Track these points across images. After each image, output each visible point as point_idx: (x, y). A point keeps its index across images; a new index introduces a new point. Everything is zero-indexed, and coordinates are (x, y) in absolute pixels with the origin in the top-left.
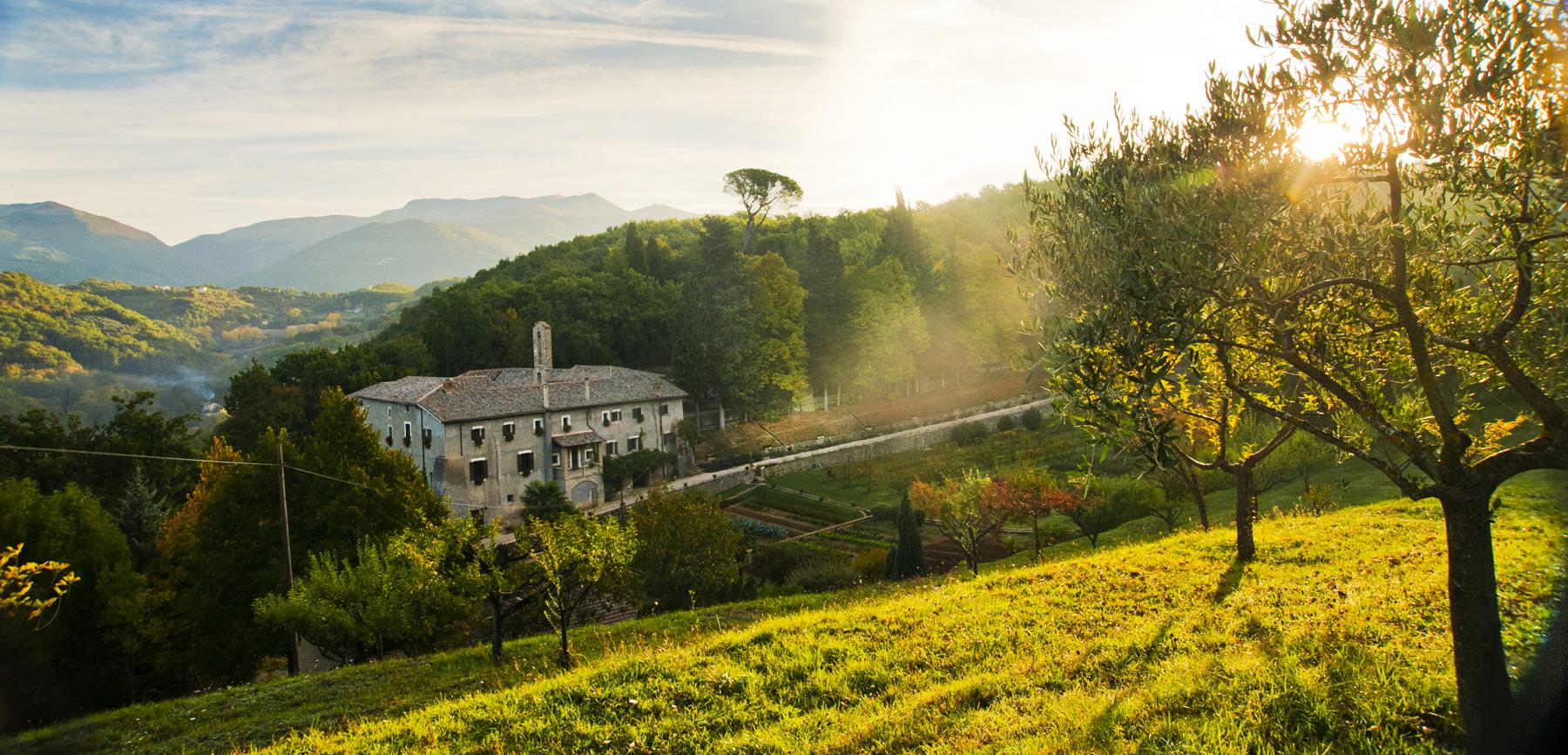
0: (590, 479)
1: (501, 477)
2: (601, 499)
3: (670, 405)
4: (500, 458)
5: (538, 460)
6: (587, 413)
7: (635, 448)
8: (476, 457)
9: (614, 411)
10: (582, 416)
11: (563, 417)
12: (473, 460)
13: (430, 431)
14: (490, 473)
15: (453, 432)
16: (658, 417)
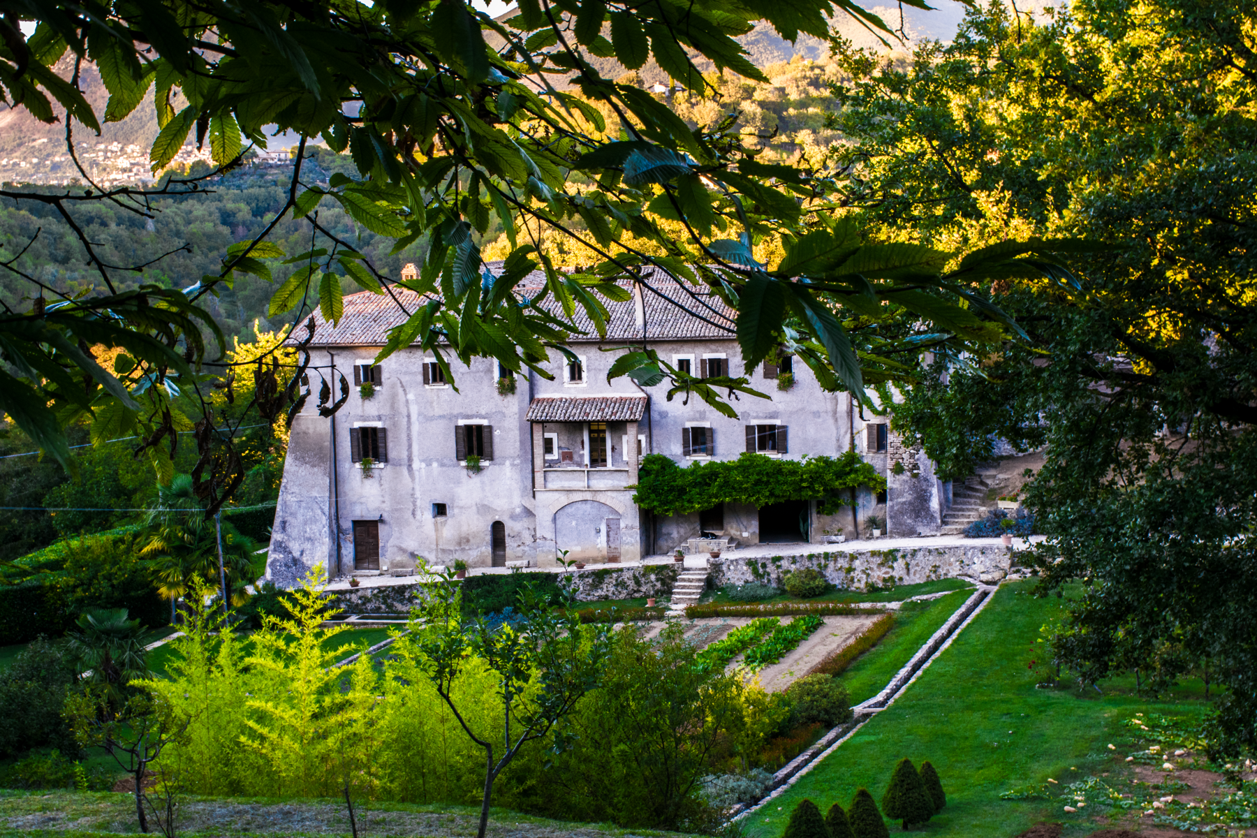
0: (601, 498)
1: (416, 465)
4: (415, 428)
5: (507, 438)
8: (364, 419)
12: (357, 425)
14: (392, 454)
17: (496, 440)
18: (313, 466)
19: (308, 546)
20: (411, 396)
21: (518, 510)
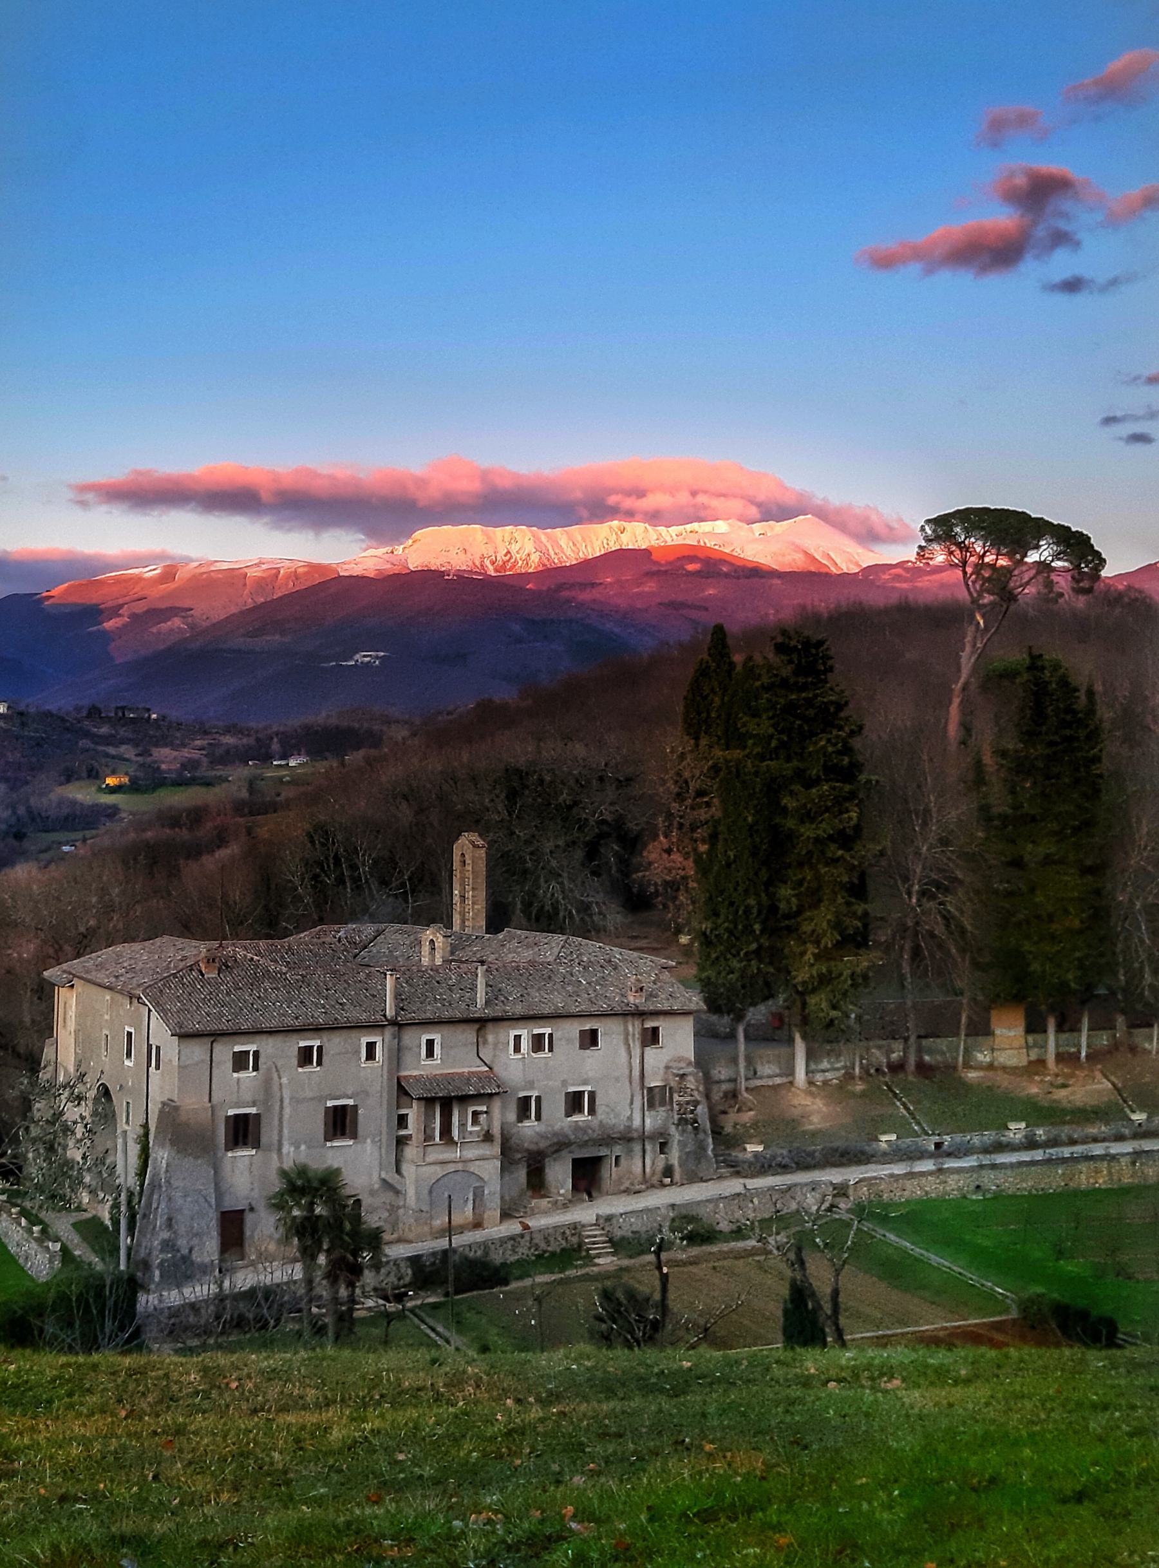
0: (472, 1168)
1: (285, 1150)
2: (493, 1212)
3: (664, 1026)
4: (287, 1111)
6: (479, 1030)
7: (581, 1111)
8: (238, 1105)
9: (536, 1031)
10: (468, 1034)
11: (425, 1037)
12: (231, 1112)
13: (158, 1048)
14: (264, 1140)
15: (197, 1051)
16: (636, 1052)
17: (361, 1119)
18: (196, 1158)
19: (195, 1241)
20: (284, 1080)
21: (376, 1186)
